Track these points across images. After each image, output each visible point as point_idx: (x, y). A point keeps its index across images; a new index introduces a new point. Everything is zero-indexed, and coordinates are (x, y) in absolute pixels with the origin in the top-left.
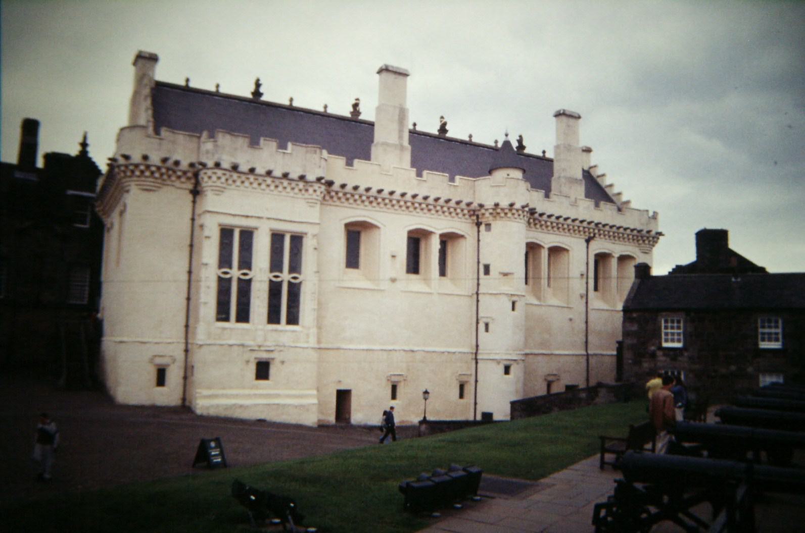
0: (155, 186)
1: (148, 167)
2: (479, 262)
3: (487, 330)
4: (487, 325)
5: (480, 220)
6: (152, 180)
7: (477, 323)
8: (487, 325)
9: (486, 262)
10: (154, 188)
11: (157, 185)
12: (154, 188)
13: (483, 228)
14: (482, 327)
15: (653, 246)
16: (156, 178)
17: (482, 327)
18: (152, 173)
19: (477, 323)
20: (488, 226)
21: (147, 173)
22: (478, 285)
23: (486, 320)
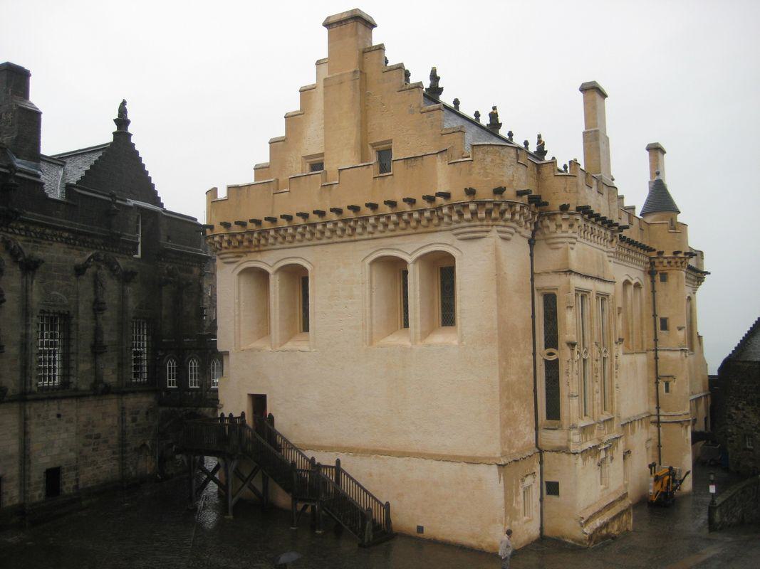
0: (482, 231)
1: (481, 204)
2: (655, 315)
3: (667, 391)
4: (667, 384)
5: (655, 269)
6: (478, 223)
7: (657, 383)
8: (667, 384)
9: (664, 316)
10: (481, 235)
11: (484, 228)
12: (481, 235)
13: (658, 278)
14: (662, 385)
15: (699, 285)
16: (481, 220)
17: (662, 385)
18: (489, 212)
19: (657, 383)
20: (664, 278)
21: (482, 214)
22: (656, 340)
23: (666, 379)
